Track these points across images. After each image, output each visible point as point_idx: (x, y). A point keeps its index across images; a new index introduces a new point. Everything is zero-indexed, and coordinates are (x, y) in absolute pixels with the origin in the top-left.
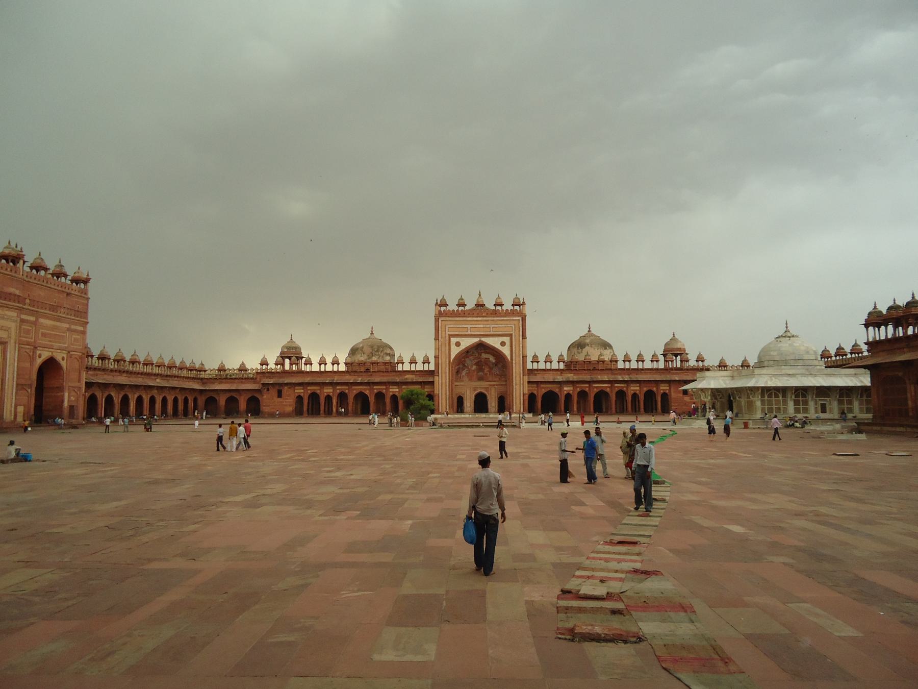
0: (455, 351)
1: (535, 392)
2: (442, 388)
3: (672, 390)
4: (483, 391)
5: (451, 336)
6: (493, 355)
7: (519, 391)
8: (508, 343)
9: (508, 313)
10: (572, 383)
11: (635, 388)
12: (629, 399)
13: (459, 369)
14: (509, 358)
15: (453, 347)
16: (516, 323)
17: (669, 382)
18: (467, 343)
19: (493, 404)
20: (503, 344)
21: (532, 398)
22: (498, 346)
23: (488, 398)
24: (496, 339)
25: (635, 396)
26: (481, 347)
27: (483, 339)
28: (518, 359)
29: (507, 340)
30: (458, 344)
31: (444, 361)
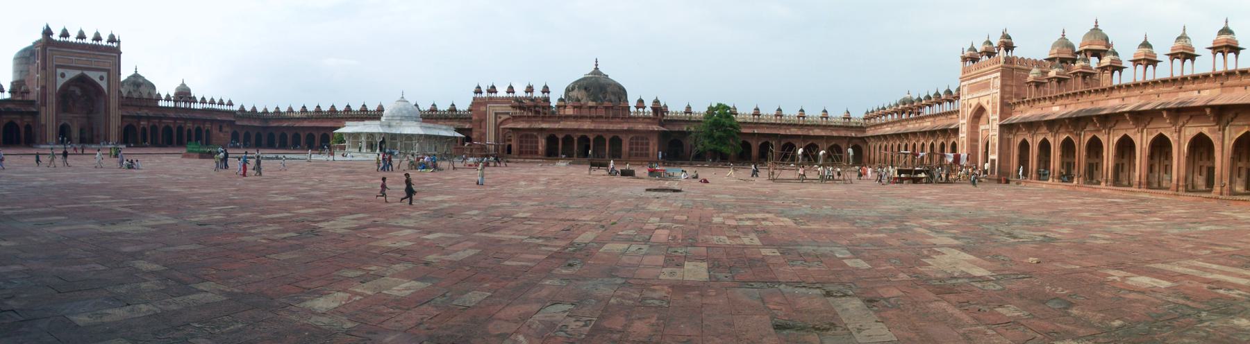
0: (60, 82)
7: (115, 125)
9: (107, 49)
10: (148, 118)
11: (189, 125)
12: (185, 133)
15: (59, 78)
17: (212, 121)
18: (71, 74)
20: (101, 78)
22: (97, 80)
25: (189, 131)
26: (82, 81)
27: (86, 72)
29: (104, 74)
30: (63, 75)
31: (50, 89)
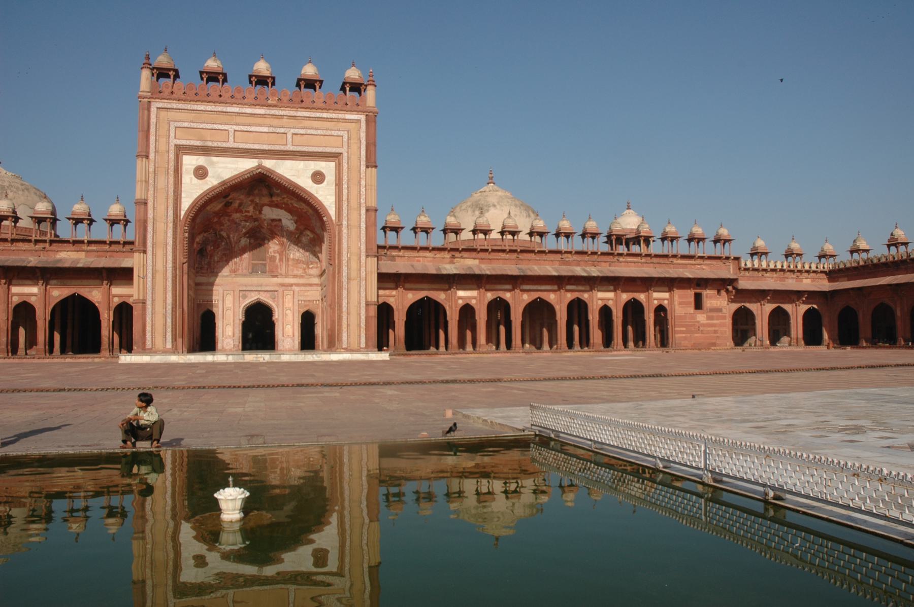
0: (193, 191)
1: (391, 301)
2: (155, 285)
3: (676, 298)
4: (266, 299)
5: (181, 150)
6: (290, 210)
8: (330, 177)
12: (594, 317)
13: (205, 242)
14: (332, 212)
16: (352, 126)
19: (289, 329)
20: (318, 177)
21: (384, 313)
22: (304, 182)
23: (277, 316)
24: (300, 165)
27: (269, 164)
28: (354, 216)
30: (201, 173)
